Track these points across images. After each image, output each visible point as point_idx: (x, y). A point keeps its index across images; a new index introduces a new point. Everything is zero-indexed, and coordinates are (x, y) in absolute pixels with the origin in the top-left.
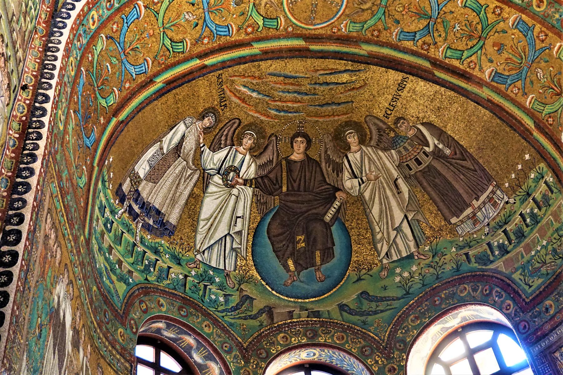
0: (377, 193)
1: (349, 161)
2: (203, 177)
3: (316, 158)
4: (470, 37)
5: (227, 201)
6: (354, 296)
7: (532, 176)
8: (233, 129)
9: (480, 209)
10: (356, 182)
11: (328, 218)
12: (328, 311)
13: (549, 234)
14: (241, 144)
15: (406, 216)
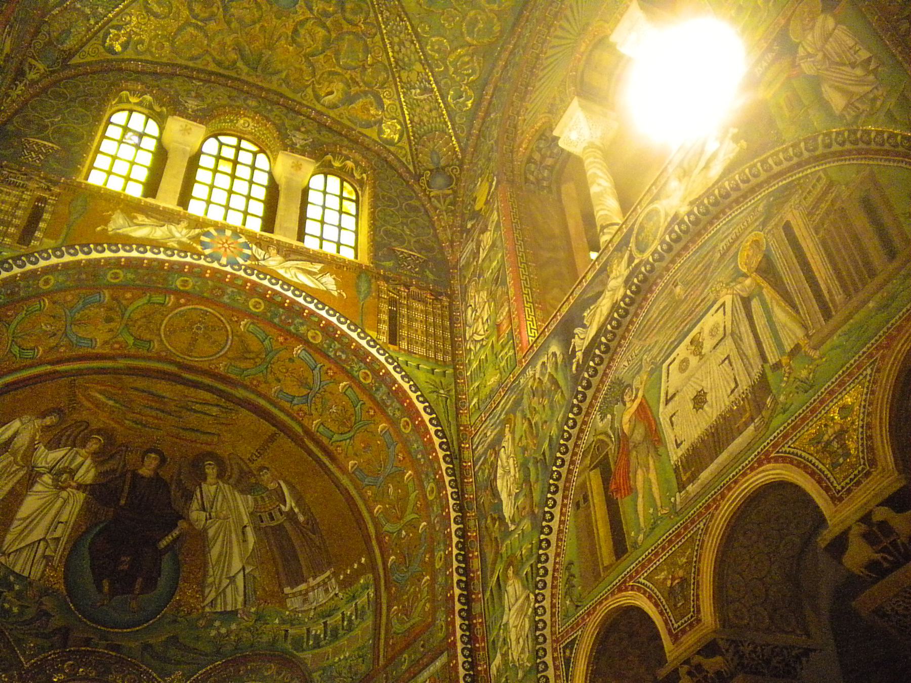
0: (222, 534)
1: (201, 491)
2: (31, 475)
3: (167, 478)
4: (344, 424)
5: (52, 503)
6: (163, 638)
7: (362, 581)
8: (78, 430)
9: (313, 589)
10: (203, 514)
11: (163, 544)
12: (130, 648)
13: (354, 647)
14: (84, 447)
15: (244, 569)
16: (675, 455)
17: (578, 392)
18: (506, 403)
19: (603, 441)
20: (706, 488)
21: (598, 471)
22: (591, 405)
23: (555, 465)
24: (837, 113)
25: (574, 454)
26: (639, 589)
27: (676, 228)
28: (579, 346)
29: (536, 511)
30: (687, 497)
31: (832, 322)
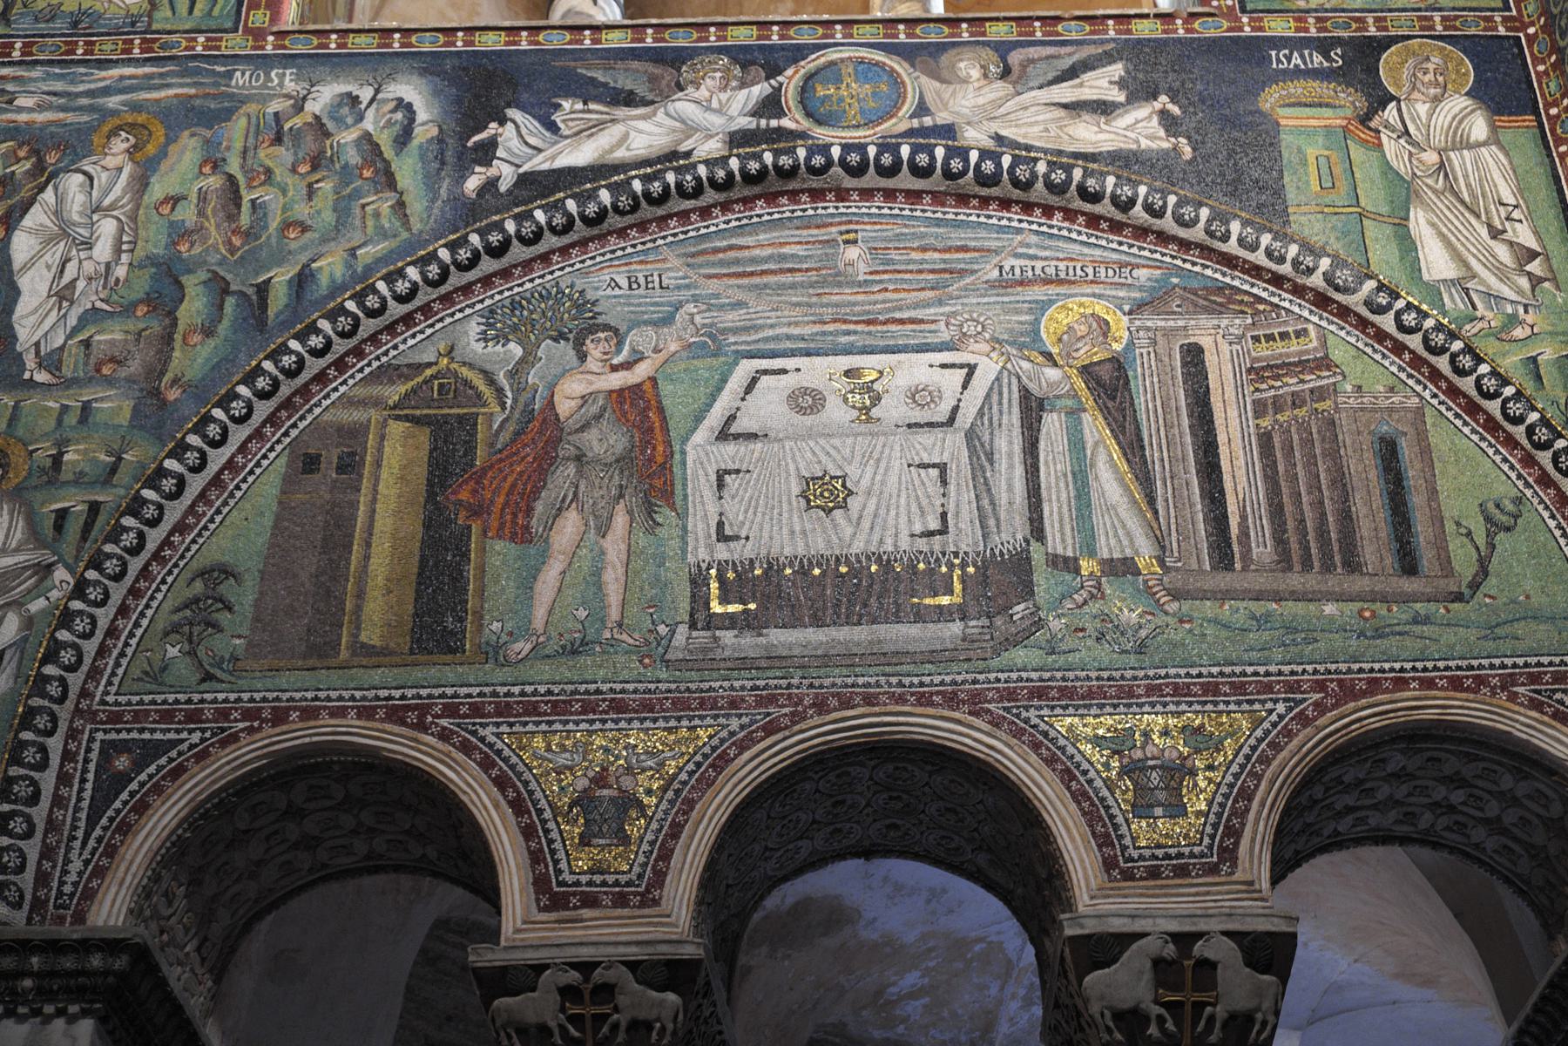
16: (702, 550)
17: (464, 241)
18: (146, 83)
19: (467, 384)
20: (775, 660)
21: (424, 437)
22: (466, 290)
23: (302, 337)
24: (1426, 277)
25: (358, 352)
26: (466, 748)
27: (940, 152)
28: (508, 150)
29: (173, 395)
30: (705, 650)
31: (1224, 580)
